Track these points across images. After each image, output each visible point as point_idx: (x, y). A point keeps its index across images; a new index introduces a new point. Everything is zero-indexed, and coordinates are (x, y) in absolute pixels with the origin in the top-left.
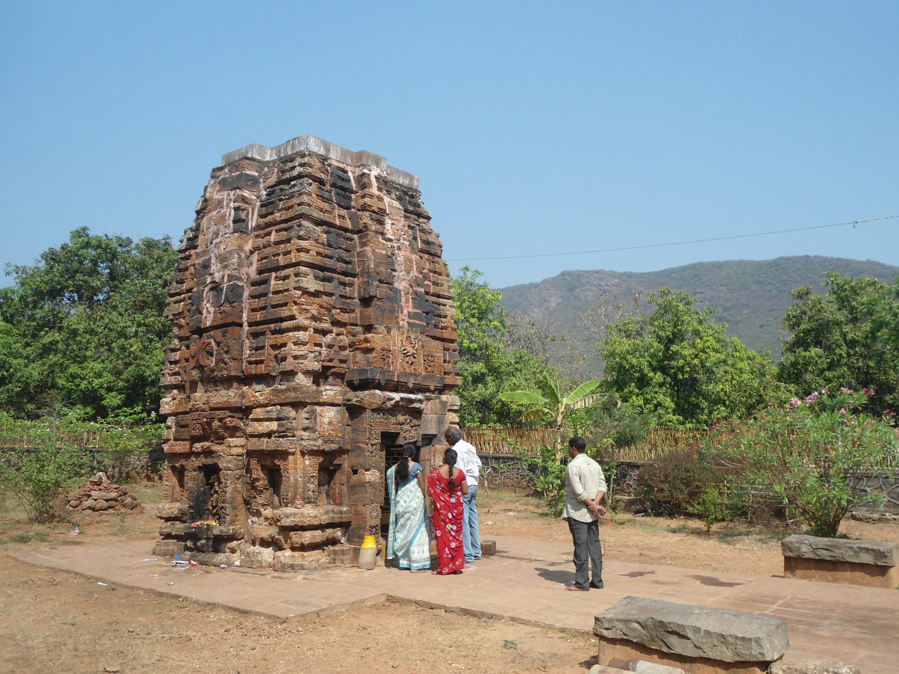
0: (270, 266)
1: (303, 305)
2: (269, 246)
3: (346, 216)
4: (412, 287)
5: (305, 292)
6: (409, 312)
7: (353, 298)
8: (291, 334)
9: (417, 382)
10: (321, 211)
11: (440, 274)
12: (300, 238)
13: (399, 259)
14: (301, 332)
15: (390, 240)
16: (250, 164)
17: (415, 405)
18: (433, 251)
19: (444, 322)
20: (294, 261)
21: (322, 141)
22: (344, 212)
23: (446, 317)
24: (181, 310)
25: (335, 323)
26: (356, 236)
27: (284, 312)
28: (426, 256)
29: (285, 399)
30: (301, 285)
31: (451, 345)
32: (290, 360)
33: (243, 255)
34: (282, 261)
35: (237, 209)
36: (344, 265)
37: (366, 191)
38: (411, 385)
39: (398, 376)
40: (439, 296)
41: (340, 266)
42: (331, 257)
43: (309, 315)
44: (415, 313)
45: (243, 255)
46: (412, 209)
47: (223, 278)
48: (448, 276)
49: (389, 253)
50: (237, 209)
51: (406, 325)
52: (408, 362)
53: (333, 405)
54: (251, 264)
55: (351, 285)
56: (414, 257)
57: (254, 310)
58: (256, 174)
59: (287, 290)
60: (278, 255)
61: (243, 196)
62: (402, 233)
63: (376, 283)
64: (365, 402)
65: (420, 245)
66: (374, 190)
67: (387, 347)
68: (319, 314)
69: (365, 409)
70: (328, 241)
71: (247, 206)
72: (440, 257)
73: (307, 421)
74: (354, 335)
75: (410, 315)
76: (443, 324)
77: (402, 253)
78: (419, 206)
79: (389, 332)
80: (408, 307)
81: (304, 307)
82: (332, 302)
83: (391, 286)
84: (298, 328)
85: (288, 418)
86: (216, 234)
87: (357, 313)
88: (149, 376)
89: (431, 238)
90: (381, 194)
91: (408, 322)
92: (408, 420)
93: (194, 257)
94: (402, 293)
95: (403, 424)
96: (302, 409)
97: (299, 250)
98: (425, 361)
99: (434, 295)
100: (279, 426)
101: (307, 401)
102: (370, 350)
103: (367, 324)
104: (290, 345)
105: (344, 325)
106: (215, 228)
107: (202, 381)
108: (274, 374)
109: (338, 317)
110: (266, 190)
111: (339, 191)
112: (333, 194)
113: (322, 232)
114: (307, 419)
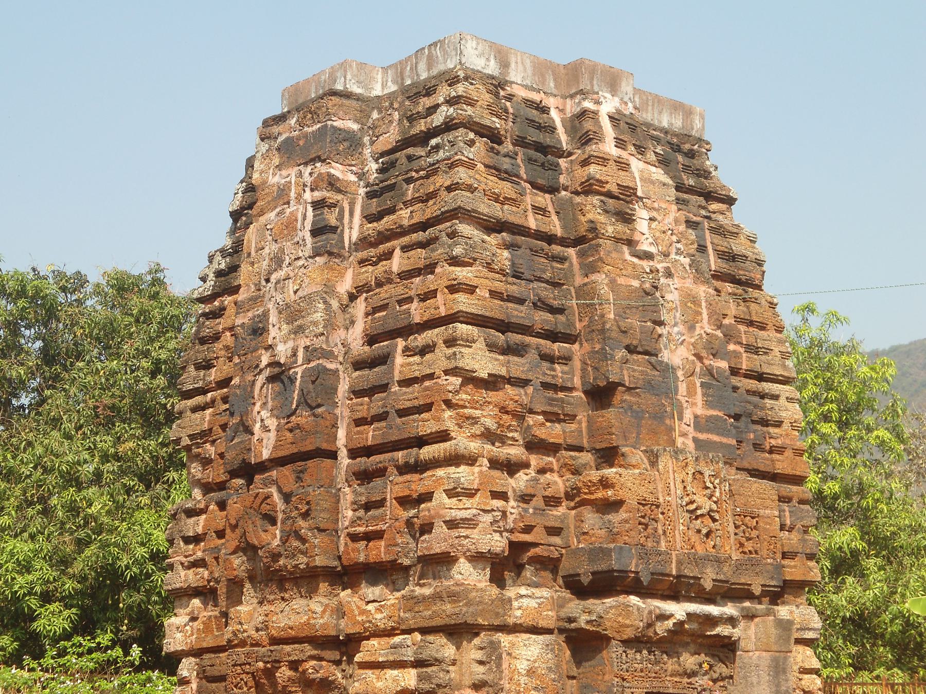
0: (392, 325)
1: (465, 407)
2: (390, 281)
3: (550, 208)
5: (470, 380)
6: (696, 417)
7: (570, 389)
8: (440, 472)
9: (722, 577)
10: (497, 200)
11: (763, 328)
12: (455, 261)
13: (669, 297)
14: (463, 468)
15: (648, 256)
16: (341, 105)
18: (742, 274)
19: (777, 436)
20: (443, 312)
21: (492, 45)
22: (544, 200)
23: (778, 424)
24: (206, 426)
25: (535, 445)
26: (571, 252)
27: (426, 425)
28: (729, 287)
29: (431, 618)
30: (460, 365)
31: (795, 488)
32: (440, 529)
33: (335, 304)
34: (417, 312)
35: (318, 205)
36: (548, 316)
37: (592, 149)
38: (708, 585)
39: (679, 563)
41: (541, 318)
42: (521, 301)
43: (477, 429)
44: (709, 419)
45: (335, 304)
46: (691, 182)
47: (294, 355)
48: (779, 329)
49: (647, 286)
50: (318, 205)
51: (691, 445)
52: (699, 531)
53: (535, 630)
54: (353, 322)
55: (566, 359)
56: (703, 291)
57: (360, 422)
58: (355, 127)
59: (431, 376)
60: (409, 300)
61: (329, 175)
62: (674, 238)
63: (621, 354)
64: (608, 624)
65: (713, 262)
66: (609, 147)
67: (651, 498)
69: (608, 639)
70: (513, 264)
71: (339, 197)
72: (759, 287)
73: (481, 669)
74: (576, 472)
75: (700, 424)
76: (773, 442)
77: (676, 282)
78: (706, 174)
79: (654, 463)
80: (694, 404)
81: (467, 411)
82: (526, 400)
83: (653, 359)
84: (455, 460)
85: (438, 661)
86: (277, 261)
87: (580, 423)
88: (127, 567)
89: (738, 246)
90: (624, 154)
91: (695, 440)
92: (706, 666)
93: (231, 311)
94: (680, 373)
95: (693, 674)
96: (470, 641)
97: (453, 289)
98: (737, 527)
100: (420, 678)
101: (480, 621)
102: (614, 505)
103: (604, 445)
104: (440, 498)
105: (550, 448)
106: (275, 247)
107: (252, 579)
108: (406, 562)
109: (541, 433)
110: (376, 160)
111: (531, 152)
112: (519, 161)
113: (499, 246)
114: (481, 663)
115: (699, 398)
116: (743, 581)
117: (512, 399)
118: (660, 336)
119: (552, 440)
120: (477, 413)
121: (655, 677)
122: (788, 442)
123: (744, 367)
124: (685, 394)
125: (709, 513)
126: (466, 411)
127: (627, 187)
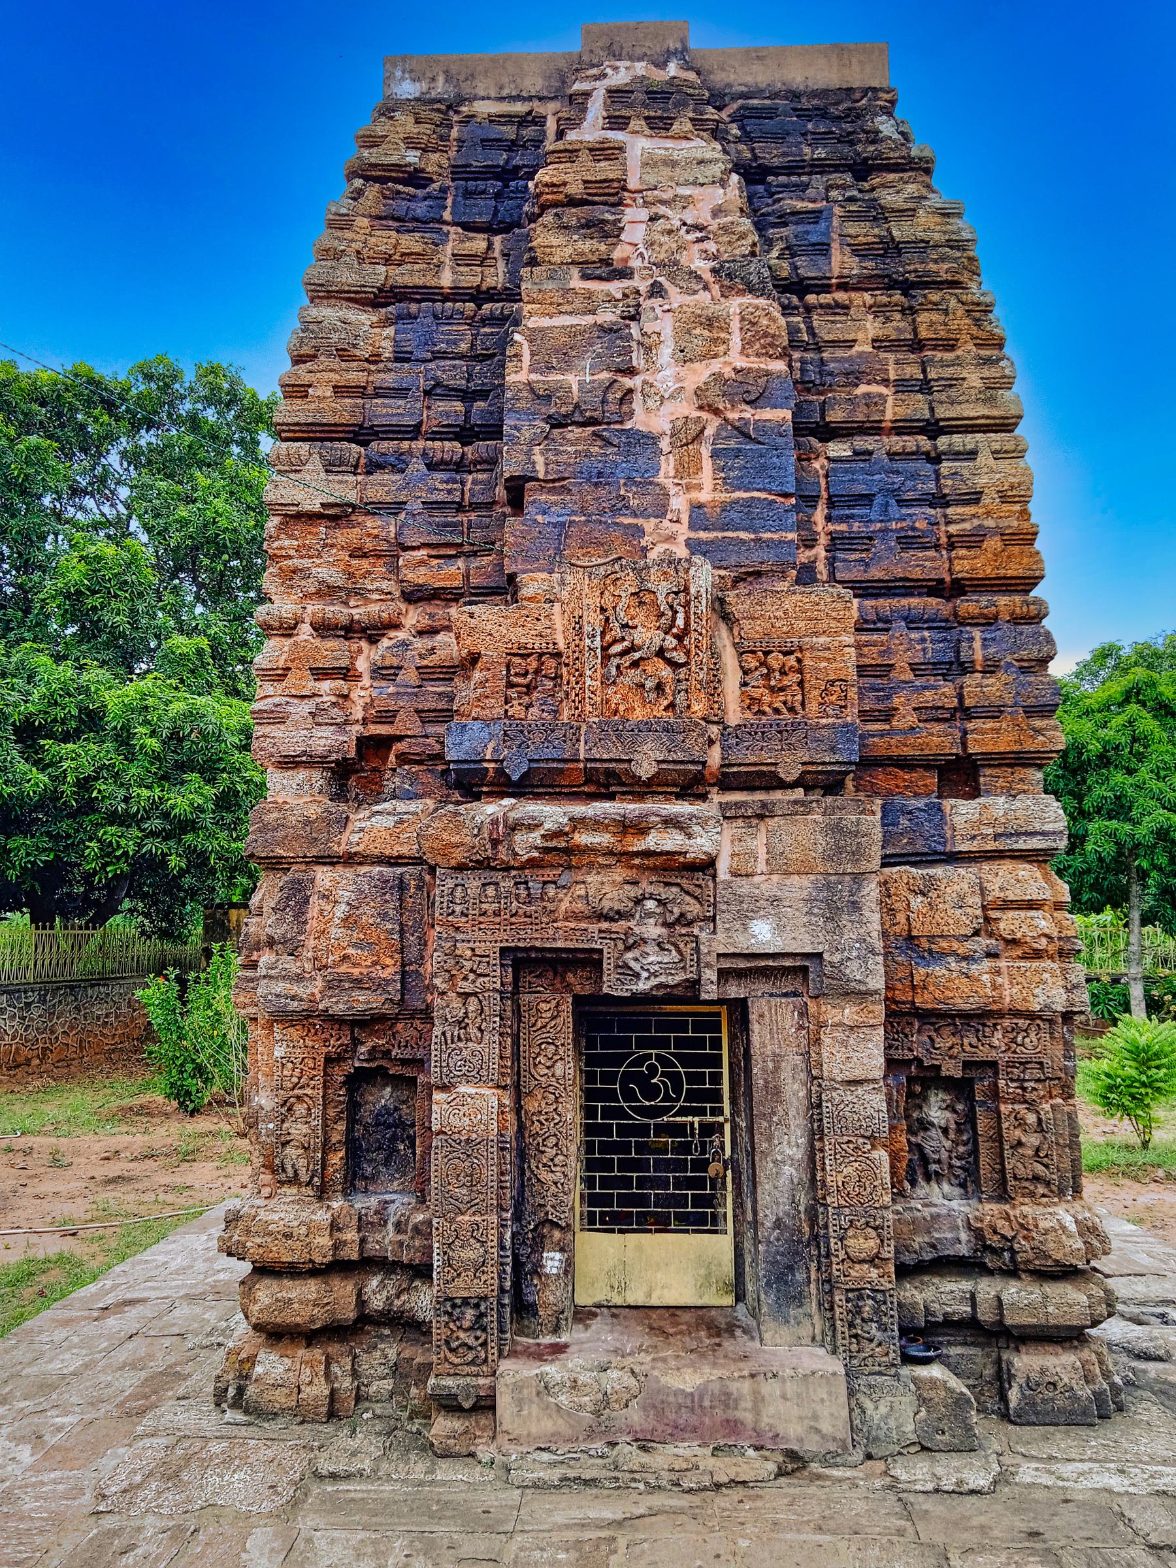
1: (290, 557)
4: (716, 412)
9: (680, 756)
17: (652, 841)
23: (974, 498)
25: (414, 596)
31: (1003, 600)
40: (933, 429)
42: (400, 392)
44: (726, 507)
46: (821, 153)
51: (682, 552)
67: (537, 644)
68: (351, 576)
75: (699, 515)
76: (952, 529)
91: (688, 543)
94: (664, 444)
98: (746, 673)
99: (901, 428)
101: (280, 852)
115: (707, 475)
116: (753, 759)
117: (369, 535)
118: (630, 391)
119: (441, 584)
120: (306, 562)
121: (525, 923)
122: (990, 523)
123: (889, 415)
124: (672, 473)
125: (661, 653)
126: (290, 562)
127: (604, 181)
